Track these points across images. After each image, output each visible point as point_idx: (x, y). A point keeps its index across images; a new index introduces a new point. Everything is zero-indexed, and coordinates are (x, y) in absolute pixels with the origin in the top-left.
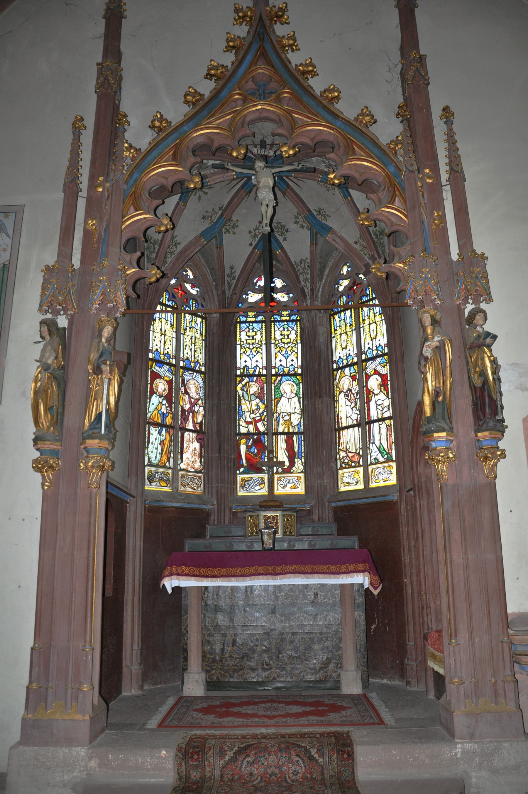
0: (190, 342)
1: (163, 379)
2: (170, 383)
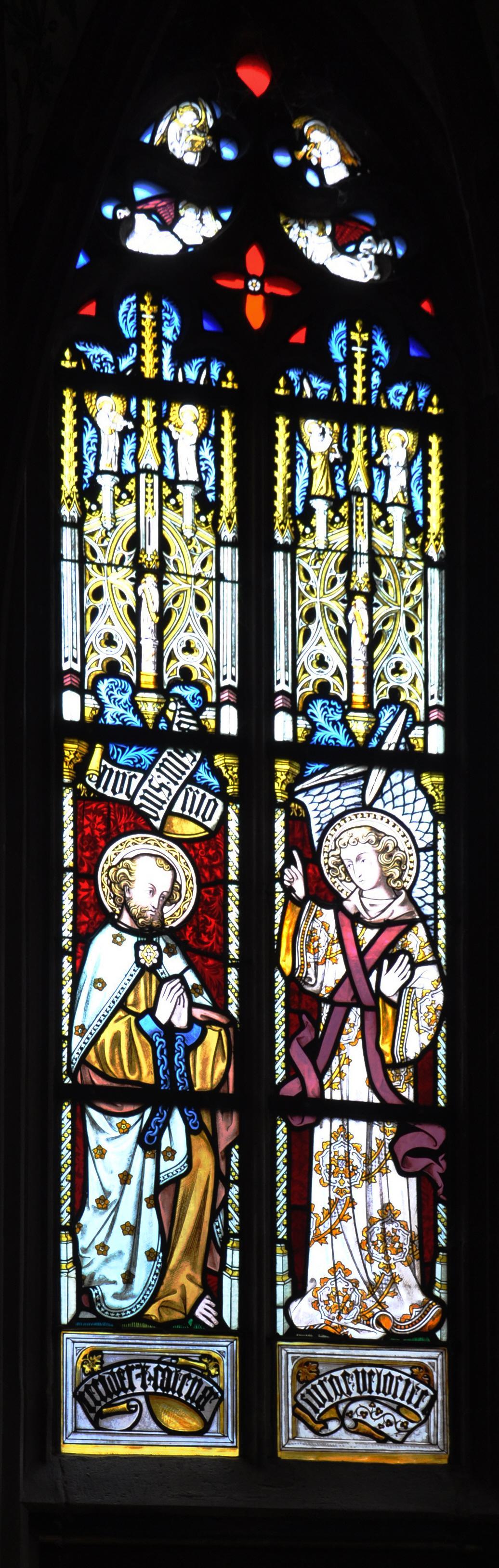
0: (339, 588)
1: (159, 832)
2: (205, 852)
